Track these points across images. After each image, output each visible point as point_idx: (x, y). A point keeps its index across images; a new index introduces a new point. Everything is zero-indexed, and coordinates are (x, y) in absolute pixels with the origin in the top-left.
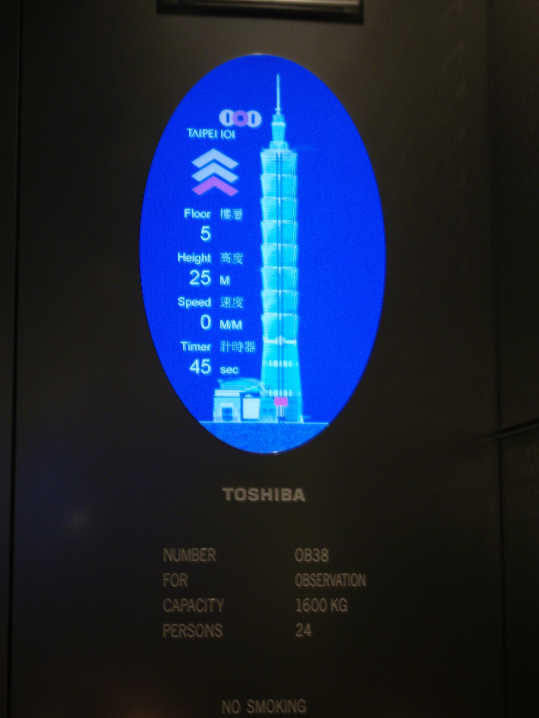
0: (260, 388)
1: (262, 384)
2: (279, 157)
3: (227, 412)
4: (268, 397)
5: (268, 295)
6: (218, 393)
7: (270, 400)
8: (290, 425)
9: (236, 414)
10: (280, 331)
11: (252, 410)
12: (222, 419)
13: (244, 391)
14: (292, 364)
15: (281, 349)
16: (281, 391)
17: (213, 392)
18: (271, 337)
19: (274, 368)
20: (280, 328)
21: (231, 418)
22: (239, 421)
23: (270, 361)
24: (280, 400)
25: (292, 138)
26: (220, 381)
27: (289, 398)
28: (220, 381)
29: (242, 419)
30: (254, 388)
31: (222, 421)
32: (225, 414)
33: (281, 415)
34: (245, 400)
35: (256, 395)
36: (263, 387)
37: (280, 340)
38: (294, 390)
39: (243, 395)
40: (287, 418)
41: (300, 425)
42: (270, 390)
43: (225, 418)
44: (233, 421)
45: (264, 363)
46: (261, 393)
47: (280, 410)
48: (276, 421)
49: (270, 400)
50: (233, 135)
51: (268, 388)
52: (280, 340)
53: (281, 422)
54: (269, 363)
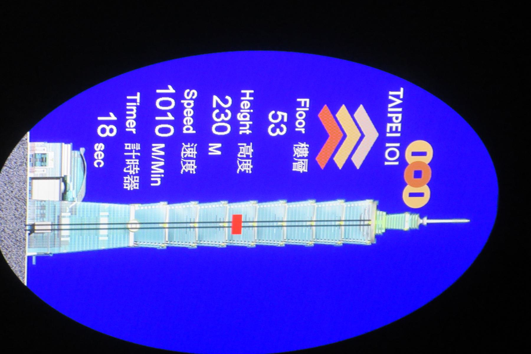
0: (73, 201)
1: (80, 204)
2: (366, 223)
3: (43, 160)
4: (61, 212)
5: (192, 210)
6: (67, 147)
7: (57, 214)
8: (24, 239)
9: (39, 171)
10: (146, 226)
11: (44, 192)
12: (33, 153)
13: (68, 181)
14: (103, 241)
16: (68, 227)
17: (67, 142)
18: (137, 216)
19: (97, 218)
20: (149, 226)
21: (33, 165)
22: (30, 175)
23: (107, 214)
24: (57, 227)
25: (390, 237)
26: (82, 150)
27: (59, 236)
28: (82, 150)
30: (70, 194)
31: (29, 153)
32: (38, 157)
34: (58, 181)
35: (63, 196)
36: (74, 203)
37: (134, 226)
38: (70, 243)
39: (64, 180)
40: (33, 235)
41: (24, 252)
42: (69, 214)
43: (34, 156)
45: (106, 206)
46: (65, 202)
47: (44, 225)
48: (29, 222)
49: (57, 214)
50: (391, 162)
51: (73, 211)
52: (134, 226)
53: (28, 228)
54: (106, 211)
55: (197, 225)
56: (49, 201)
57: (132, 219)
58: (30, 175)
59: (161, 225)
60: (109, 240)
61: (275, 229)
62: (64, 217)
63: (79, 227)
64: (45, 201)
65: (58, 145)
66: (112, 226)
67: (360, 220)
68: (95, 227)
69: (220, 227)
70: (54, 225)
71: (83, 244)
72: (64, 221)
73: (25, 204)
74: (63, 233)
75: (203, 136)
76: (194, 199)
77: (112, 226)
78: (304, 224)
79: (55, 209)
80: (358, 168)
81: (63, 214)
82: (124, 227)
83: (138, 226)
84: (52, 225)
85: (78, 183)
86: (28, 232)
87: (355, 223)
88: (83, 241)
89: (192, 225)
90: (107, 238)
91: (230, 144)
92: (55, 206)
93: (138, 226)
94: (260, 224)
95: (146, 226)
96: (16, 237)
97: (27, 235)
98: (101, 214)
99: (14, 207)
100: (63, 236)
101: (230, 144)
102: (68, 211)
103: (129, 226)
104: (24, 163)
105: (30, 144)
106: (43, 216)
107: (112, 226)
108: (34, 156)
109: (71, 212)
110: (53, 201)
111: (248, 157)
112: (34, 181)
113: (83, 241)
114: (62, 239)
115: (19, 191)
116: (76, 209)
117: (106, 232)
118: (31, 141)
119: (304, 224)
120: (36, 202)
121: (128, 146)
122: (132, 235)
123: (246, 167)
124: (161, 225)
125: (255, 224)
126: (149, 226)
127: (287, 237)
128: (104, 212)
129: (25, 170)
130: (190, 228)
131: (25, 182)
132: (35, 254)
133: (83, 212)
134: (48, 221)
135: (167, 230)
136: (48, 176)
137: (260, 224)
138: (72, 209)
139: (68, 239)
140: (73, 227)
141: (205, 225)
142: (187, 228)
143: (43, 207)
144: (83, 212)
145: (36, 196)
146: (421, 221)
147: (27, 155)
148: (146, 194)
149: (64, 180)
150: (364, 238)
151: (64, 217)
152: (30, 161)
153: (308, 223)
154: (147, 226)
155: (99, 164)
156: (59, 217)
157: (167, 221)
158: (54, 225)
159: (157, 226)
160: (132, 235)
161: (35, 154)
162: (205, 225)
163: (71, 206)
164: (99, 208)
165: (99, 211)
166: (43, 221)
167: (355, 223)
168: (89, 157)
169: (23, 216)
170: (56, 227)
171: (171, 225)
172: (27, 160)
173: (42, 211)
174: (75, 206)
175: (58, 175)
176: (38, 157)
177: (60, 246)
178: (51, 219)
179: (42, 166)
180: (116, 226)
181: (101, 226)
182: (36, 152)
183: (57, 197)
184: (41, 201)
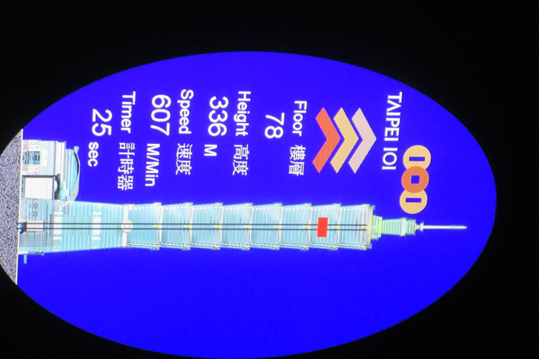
0: (66, 200)
2: (362, 227)
3: (37, 158)
4: (53, 210)
5: (186, 211)
6: (61, 145)
8: (16, 238)
9: (32, 169)
10: (139, 226)
11: (37, 190)
12: (26, 151)
13: (61, 180)
14: (96, 241)
15: (115, 226)
16: (60, 226)
17: (60, 141)
20: (143, 226)
23: (101, 213)
24: (49, 226)
25: (386, 243)
26: (76, 149)
27: (51, 235)
28: (76, 149)
29: (25, 177)
30: (64, 193)
32: (31, 155)
33: (28, 226)
34: (51, 179)
35: (56, 195)
36: (67, 202)
37: (127, 226)
38: (62, 243)
40: (24, 233)
42: (62, 213)
43: (27, 154)
44: (22, 165)
46: (58, 201)
47: (35, 224)
48: (21, 220)
50: (389, 166)
51: (65, 210)
52: (127, 226)
53: (19, 226)
54: (99, 211)
55: (191, 227)
56: (42, 199)
57: (126, 220)
58: (23, 173)
59: (154, 226)
60: (102, 240)
61: (270, 232)
62: (57, 216)
63: (71, 226)
64: (37, 200)
65: (52, 143)
66: (105, 226)
67: (357, 225)
68: (88, 226)
69: (214, 229)
70: (47, 224)
71: (75, 243)
72: (56, 220)
73: (18, 202)
74: (55, 232)
75: (199, 136)
76: (189, 201)
77: (105, 227)
78: (300, 227)
79: (47, 208)
80: (355, 172)
81: (55, 213)
82: (118, 227)
83: (132, 226)
84: (44, 224)
85: (71, 182)
86: (20, 230)
87: (351, 227)
88: (75, 240)
89: (186, 226)
90: (99, 238)
91: (227, 144)
92: (47, 205)
93: (132, 226)
94: (255, 227)
95: (139, 226)
96: (8, 235)
97: (19, 233)
98: (94, 213)
99: (6, 205)
100: (56, 236)
101: (227, 144)
102: (60, 210)
103: (122, 226)
104: (17, 161)
105: (23, 142)
106: (35, 214)
107: (105, 226)
108: (27, 154)
109: (64, 210)
110: (46, 200)
111: (244, 159)
112: (27, 179)
113: (75, 240)
114: (54, 238)
115: (12, 189)
116: (68, 208)
117: (98, 232)
118: (24, 138)
119: (300, 227)
120: (28, 201)
121: (122, 145)
122: (125, 235)
123: (242, 169)
124: (154, 226)
125: (250, 227)
126: (143, 226)
127: (282, 240)
128: (97, 211)
129: (18, 168)
130: (184, 229)
131: (17, 180)
132: (27, 252)
133: (76, 211)
134: (41, 220)
135: (161, 231)
136: (41, 174)
137: (255, 227)
138: (64, 208)
139: (61, 238)
140: (66, 226)
141: (199, 227)
142: (181, 229)
143: (35, 206)
144: (76, 211)
145: (28, 195)
146: (417, 227)
147: (20, 152)
148: (140, 195)
149: (57, 178)
150: (360, 242)
151: (57, 216)
152: (23, 159)
153: (304, 227)
154: (140, 226)
155: (93, 163)
156: (51, 216)
157: (161, 222)
158: (47, 224)
159: (150, 226)
160: (125, 235)
161: (29, 152)
162: (199, 227)
163: (64, 204)
164: (92, 208)
165: (92, 211)
166: (35, 219)
167: (351, 227)
168: (83, 156)
169: (15, 214)
170: (48, 226)
171: (165, 227)
172: (20, 158)
173: (34, 210)
174: (68, 205)
175: (52, 174)
176: (31, 155)
177: (52, 246)
178: (44, 218)
179: (35, 164)
180: (108, 226)
181: (94, 226)
182: (30, 150)
183: (49, 195)
184: (34, 199)
